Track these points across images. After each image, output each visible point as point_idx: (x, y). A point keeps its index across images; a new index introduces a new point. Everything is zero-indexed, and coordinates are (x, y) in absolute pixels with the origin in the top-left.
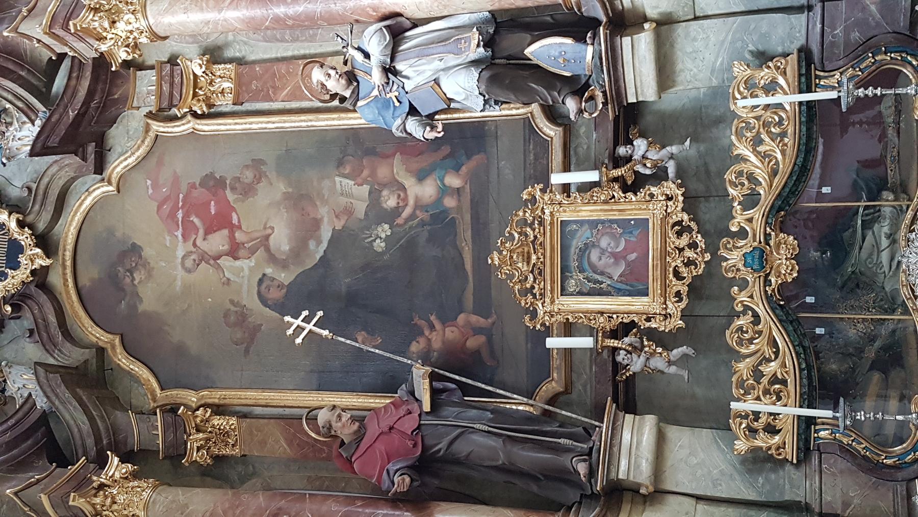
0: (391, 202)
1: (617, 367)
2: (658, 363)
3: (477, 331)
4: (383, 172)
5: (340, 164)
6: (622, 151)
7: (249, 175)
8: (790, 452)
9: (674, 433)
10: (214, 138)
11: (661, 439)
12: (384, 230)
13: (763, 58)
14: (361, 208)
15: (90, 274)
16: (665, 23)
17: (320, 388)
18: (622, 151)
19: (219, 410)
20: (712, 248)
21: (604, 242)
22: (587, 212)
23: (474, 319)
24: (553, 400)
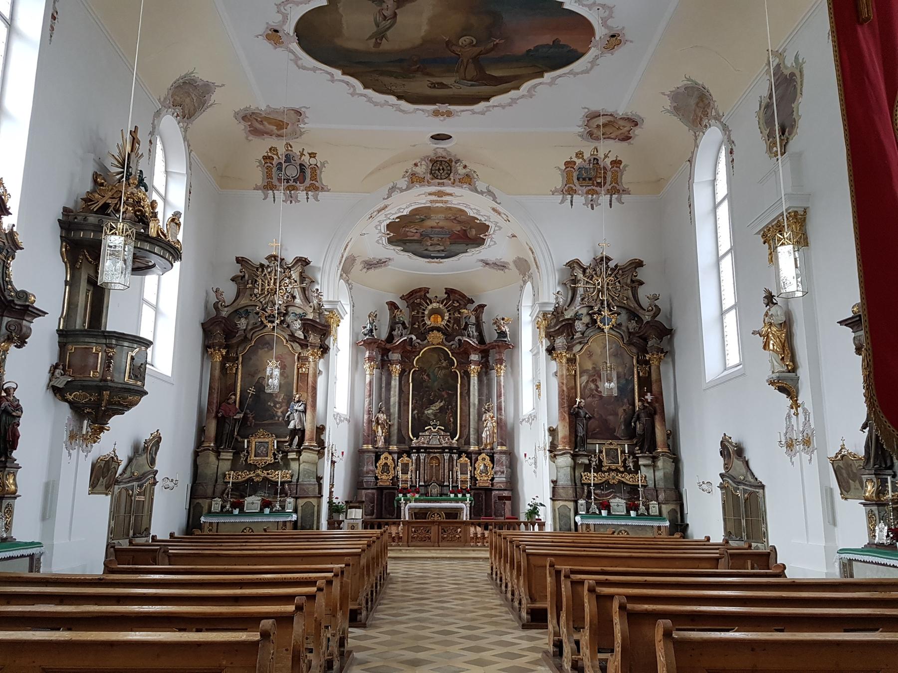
0: (277, 406)
1: (242, 452)
2: (242, 459)
3: (251, 424)
4: (284, 404)
5: (286, 395)
6: (280, 452)
7: (285, 375)
8: (226, 480)
9: (230, 461)
10: (294, 366)
11: (229, 460)
12: (272, 405)
13: (292, 476)
14: (277, 400)
15: (267, 338)
16: (299, 459)
17: (241, 391)
18: (280, 452)
19: (237, 369)
20: (262, 468)
21: (265, 449)
22: (270, 446)
23: (253, 424)
24: (236, 439)
